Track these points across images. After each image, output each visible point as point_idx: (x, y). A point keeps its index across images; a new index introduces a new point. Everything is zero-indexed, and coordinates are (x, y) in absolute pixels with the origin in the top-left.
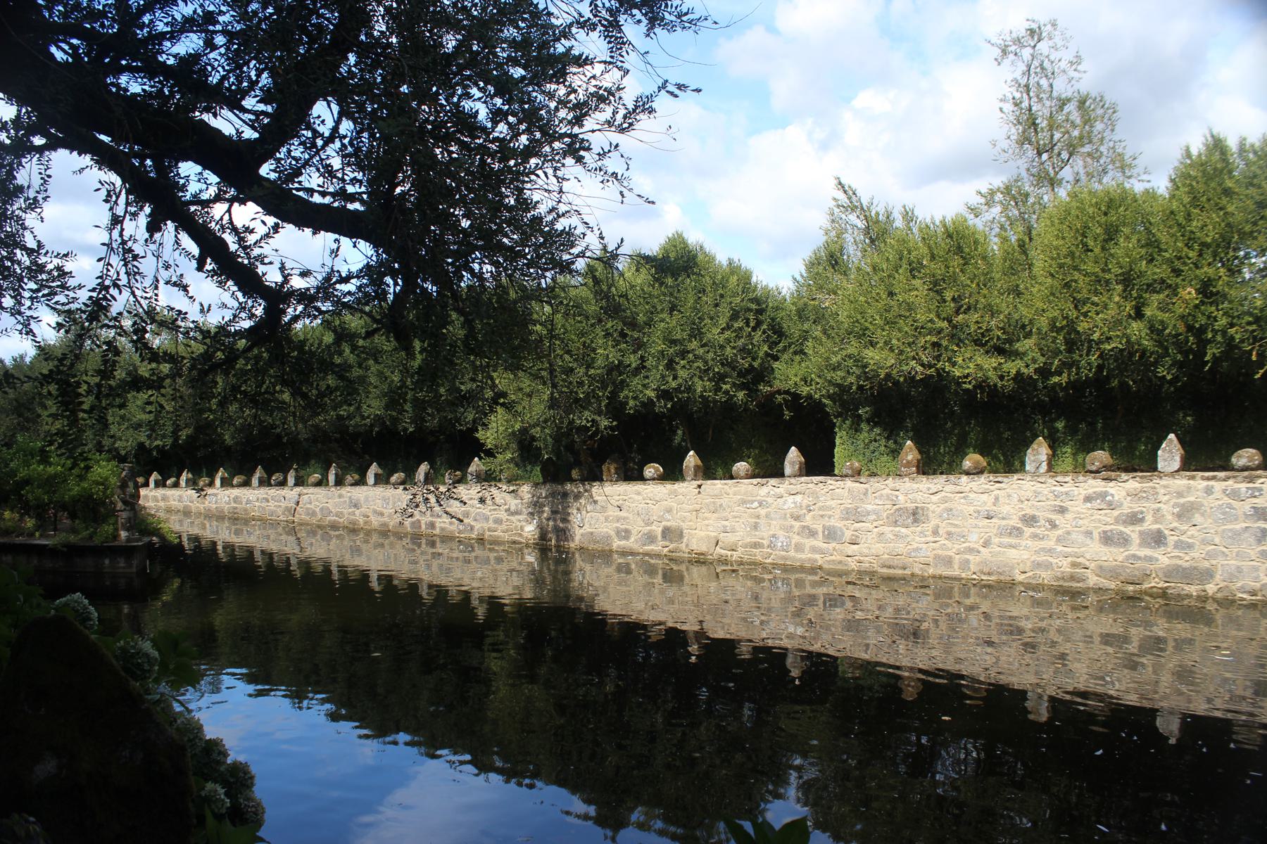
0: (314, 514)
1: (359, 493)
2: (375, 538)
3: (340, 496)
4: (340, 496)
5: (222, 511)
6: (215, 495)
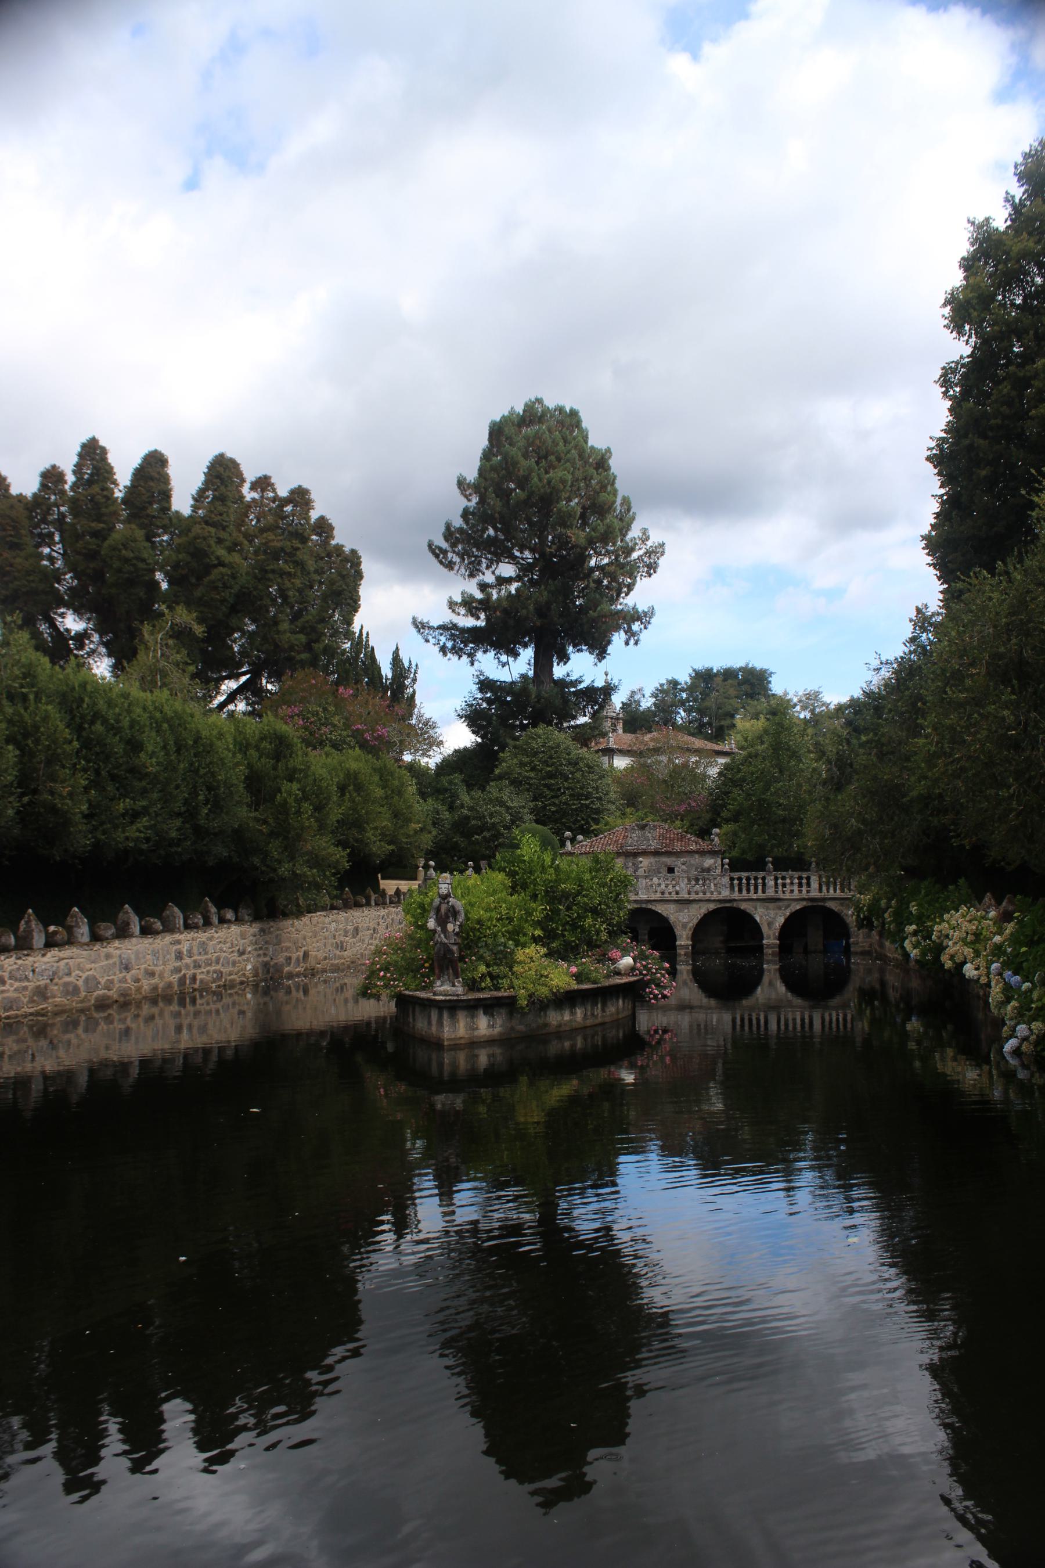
0: (76, 990)
1: (119, 949)
2: (146, 1009)
3: (108, 956)
4: (108, 956)
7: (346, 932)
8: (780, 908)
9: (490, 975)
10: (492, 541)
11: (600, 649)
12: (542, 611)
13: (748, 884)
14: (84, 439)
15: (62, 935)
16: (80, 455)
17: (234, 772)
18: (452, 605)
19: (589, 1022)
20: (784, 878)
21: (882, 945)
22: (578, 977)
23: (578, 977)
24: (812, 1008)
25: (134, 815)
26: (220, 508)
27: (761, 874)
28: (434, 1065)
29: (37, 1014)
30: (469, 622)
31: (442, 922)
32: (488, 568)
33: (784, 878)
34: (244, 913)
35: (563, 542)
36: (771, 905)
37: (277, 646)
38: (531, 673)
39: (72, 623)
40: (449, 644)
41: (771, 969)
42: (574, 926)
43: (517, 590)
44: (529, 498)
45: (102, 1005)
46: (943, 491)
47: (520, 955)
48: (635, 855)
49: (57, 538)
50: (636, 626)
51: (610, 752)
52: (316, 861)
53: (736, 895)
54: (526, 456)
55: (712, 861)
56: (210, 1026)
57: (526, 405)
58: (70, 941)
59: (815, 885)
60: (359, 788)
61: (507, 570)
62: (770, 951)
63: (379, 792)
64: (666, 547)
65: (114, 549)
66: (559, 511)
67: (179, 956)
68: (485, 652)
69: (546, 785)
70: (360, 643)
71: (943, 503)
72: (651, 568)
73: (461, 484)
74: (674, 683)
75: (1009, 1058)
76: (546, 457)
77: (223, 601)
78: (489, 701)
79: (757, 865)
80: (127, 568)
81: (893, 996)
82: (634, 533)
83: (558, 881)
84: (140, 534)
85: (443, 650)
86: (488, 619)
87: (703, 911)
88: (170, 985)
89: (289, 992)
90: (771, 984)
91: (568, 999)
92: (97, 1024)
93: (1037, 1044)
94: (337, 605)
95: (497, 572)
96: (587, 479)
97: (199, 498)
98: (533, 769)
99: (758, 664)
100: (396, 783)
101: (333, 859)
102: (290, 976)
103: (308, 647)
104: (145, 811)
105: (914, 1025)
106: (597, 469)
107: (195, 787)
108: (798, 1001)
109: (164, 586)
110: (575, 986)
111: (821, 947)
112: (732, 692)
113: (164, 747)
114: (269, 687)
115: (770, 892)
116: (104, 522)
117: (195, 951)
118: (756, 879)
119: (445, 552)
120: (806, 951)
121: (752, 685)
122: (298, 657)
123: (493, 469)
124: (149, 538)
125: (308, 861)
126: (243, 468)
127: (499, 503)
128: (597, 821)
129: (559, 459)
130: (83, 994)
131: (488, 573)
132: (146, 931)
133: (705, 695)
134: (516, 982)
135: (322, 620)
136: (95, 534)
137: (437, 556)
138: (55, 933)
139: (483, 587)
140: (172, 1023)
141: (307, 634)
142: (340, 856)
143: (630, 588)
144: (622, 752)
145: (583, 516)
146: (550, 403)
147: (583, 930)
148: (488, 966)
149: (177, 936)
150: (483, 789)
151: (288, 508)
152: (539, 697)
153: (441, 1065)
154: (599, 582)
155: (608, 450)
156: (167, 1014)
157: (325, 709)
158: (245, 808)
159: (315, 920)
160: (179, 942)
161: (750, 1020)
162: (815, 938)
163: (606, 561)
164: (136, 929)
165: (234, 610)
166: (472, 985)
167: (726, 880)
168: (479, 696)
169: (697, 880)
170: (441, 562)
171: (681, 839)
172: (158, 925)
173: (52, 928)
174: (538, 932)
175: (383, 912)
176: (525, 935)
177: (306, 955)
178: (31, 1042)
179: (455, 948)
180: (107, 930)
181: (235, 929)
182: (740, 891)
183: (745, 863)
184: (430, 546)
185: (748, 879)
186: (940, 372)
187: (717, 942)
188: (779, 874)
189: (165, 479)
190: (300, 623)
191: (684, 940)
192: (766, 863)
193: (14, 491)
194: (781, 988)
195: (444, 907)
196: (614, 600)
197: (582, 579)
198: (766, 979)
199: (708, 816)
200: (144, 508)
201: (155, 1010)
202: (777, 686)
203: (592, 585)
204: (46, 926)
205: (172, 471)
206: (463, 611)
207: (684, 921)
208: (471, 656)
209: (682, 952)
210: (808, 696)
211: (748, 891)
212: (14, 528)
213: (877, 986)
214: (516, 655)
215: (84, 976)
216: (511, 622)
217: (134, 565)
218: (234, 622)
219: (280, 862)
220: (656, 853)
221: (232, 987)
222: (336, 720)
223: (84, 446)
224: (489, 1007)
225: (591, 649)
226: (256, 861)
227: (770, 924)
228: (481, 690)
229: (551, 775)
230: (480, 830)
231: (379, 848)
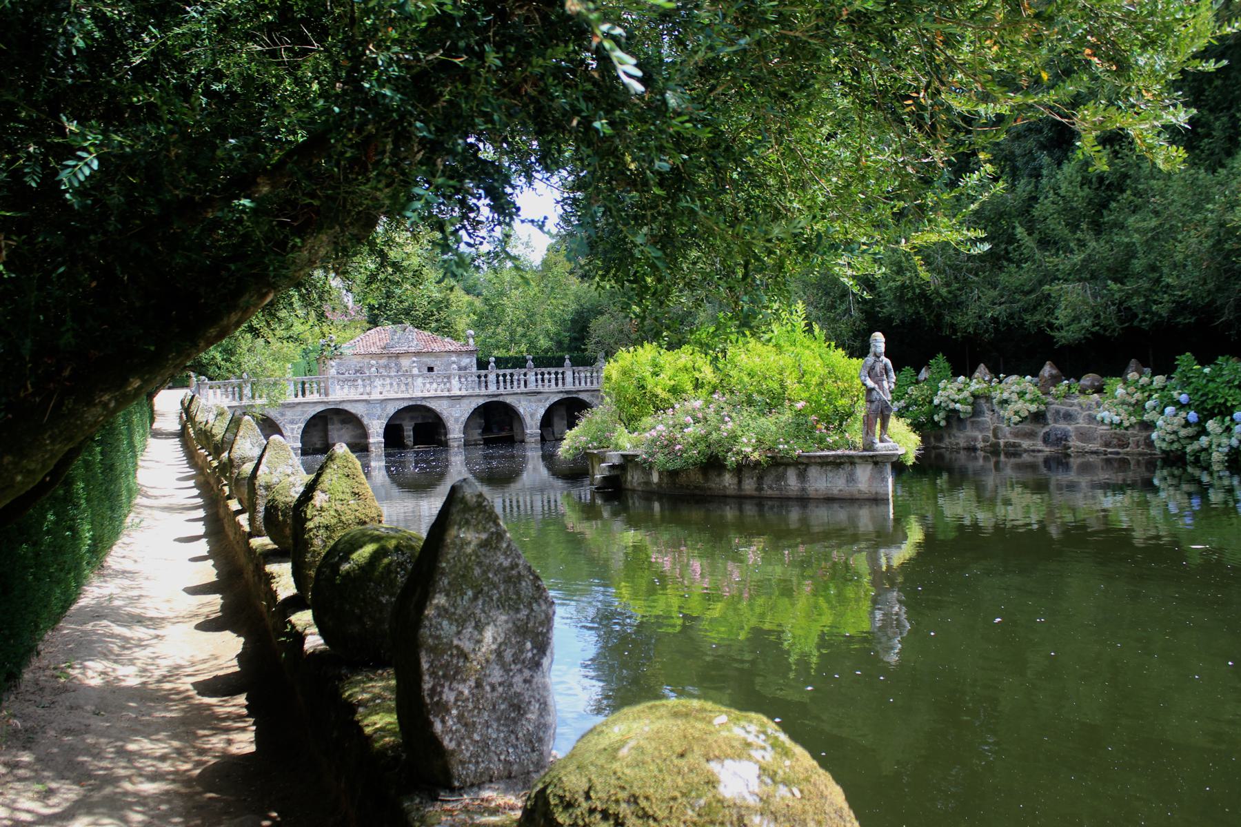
8: (540, 401)
20: (549, 373)
36: (533, 398)
53: (502, 390)
55: (468, 360)
59: (569, 378)
62: (533, 440)
87: (474, 406)
90: (535, 469)
115: (532, 387)
185: (512, 375)
188: (539, 370)
191: (455, 432)
192: (526, 361)
194: (544, 472)
198: (530, 466)
207: (456, 418)
209: (456, 444)
227: (532, 415)
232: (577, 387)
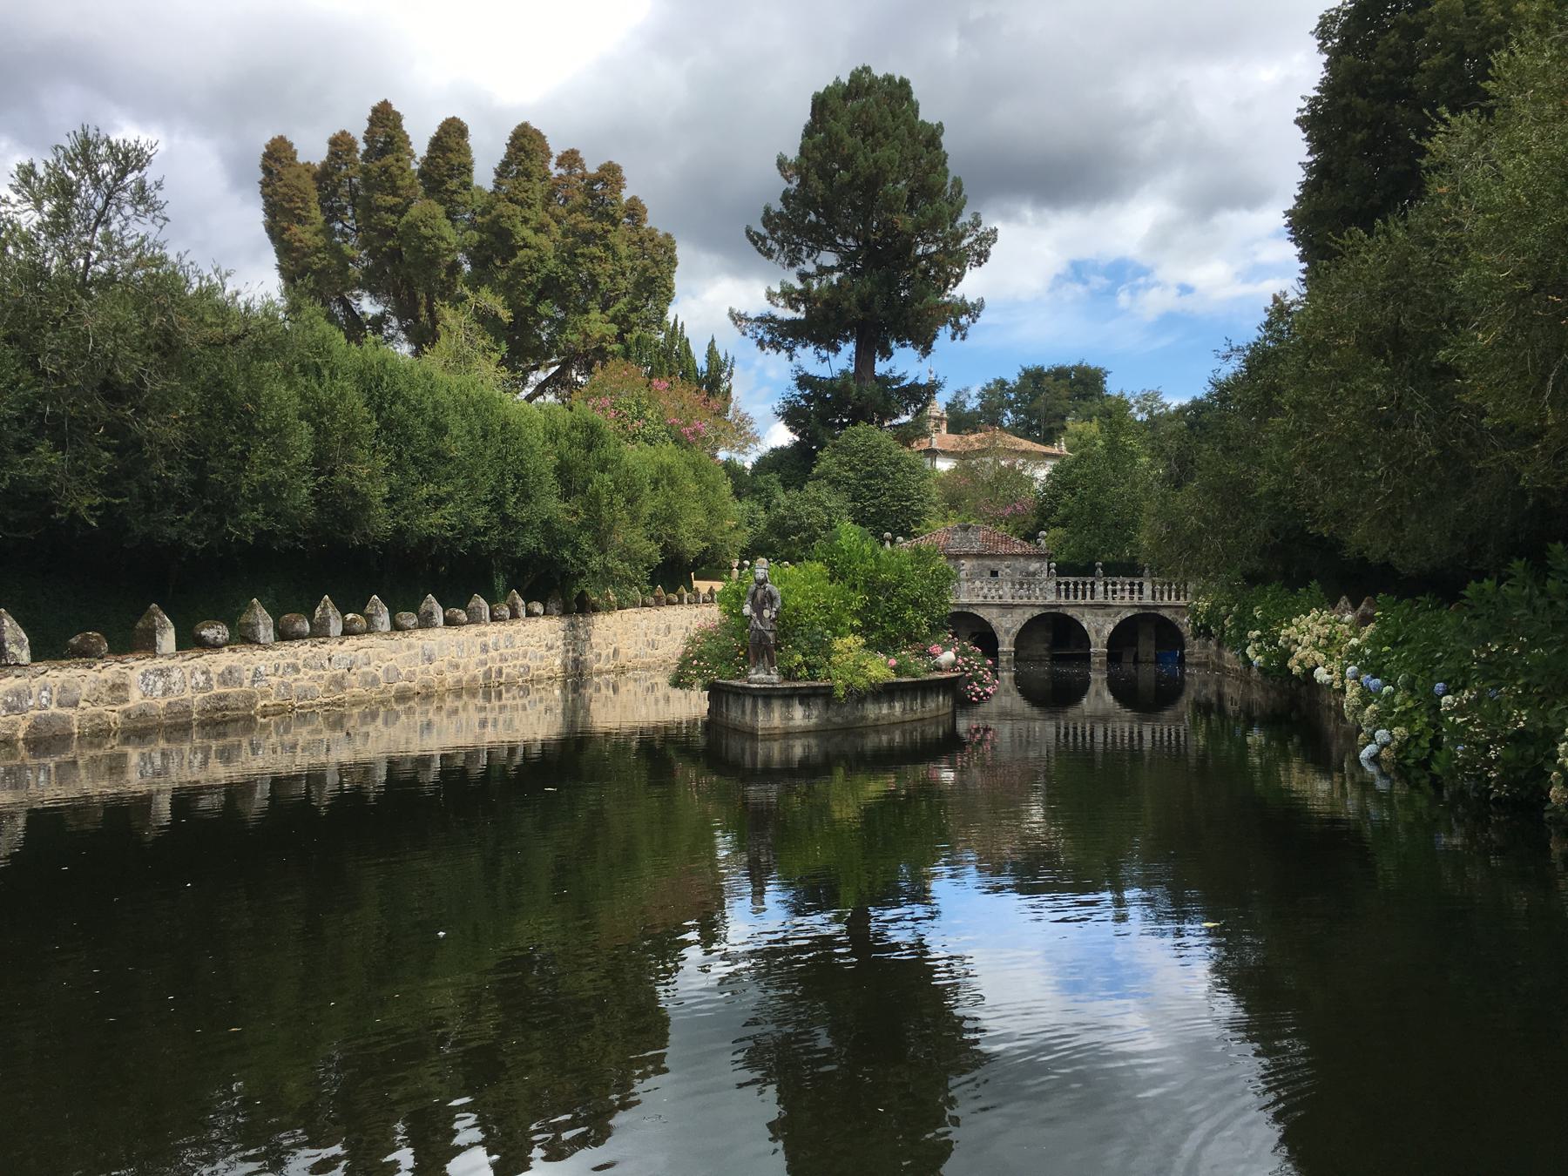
2: (450, 702)
3: (409, 647)
4: (409, 647)
5: (187, 711)
6: (161, 673)
7: (658, 629)
9: (806, 663)
10: (814, 227)
11: (924, 344)
12: (864, 304)
13: (1076, 590)
14: (375, 101)
15: (361, 622)
16: (371, 120)
17: (543, 461)
18: (770, 296)
19: (908, 717)
20: (1114, 584)
21: (1220, 656)
22: (897, 670)
23: (897, 670)
24: (1142, 720)
25: (439, 502)
26: (527, 185)
27: (1089, 580)
28: (747, 757)
29: (333, 704)
30: (787, 314)
31: (758, 608)
32: (809, 256)
33: (1114, 584)
34: (553, 606)
35: (888, 228)
36: (1100, 612)
37: (587, 335)
38: (852, 370)
39: (368, 306)
40: (767, 338)
41: (1098, 676)
42: (894, 618)
43: (839, 280)
44: (853, 179)
45: (402, 697)
46: (1310, 159)
47: (838, 644)
48: (957, 557)
49: (350, 213)
50: (963, 320)
51: (932, 453)
52: (628, 555)
53: (1063, 601)
54: (851, 133)
56: (516, 723)
57: (852, 74)
58: (370, 630)
59: (1147, 590)
60: (672, 482)
61: (829, 258)
63: (693, 487)
64: (999, 234)
65: (412, 226)
66: (886, 194)
67: (485, 649)
68: (804, 346)
69: (867, 486)
70: (675, 333)
71: (1310, 173)
72: (982, 257)
73: (781, 163)
74: (1002, 383)
75: (1364, 764)
76: (872, 134)
77: (530, 286)
78: (808, 398)
79: (1089, 570)
80: (427, 247)
81: (1231, 708)
82: (965, 218)
83: (878, 571)
84: (440, 210)
85: (761, 343)
86: (808, 311)
87: (1028, 616)
88: (474, 678)
89: (598, 690)
90: (1098, 693)
91: (887, 692)
92: (398, 717)
93: (1398, 751)
94: (652, 294)
95: (818, 261)
96: (916, 158)
97: (502, 172)
98: (852, 469)
99: (1093, 363)
100: (711, 478)
101: (646, 552)
102: (600, 673)
103: (620, 338)
104: (450, 496)
105: (1256, 737)
106: (927, 147)
107: (502, 474)
108: (1127, 714)
109: (467, 268)
110: (895, 679)
111: (1152, 657)
112: (1063, 392)
113: (469, 432)
114: (580, 379)
115: (1099, 598)
116: (400, 196)
117: (502, 643)
118: (1084, 584)
119: (764, 239)
120: (1136, 661)
121: (1086, 385)
122: (610, 348)
123: (815, 147)
124: (450, 215)
125: (620, 555)
126: (549, 140)
127: (821, 186)
128: (917, 523)
129: (887, 136)
130: (383, 685)
131: (809, 262)
132: (450, 622)
133: (1034, 396)
134: (833, 672)
135: (635, 310)
136: (391, 210)
137: (755, 243)
138: (353, 621)
139: (803, 277)
140: (476, 718)
141: (619, 324)
142: (652, 550)
143: (959, 277)
144: (946, 454)
145: (911, 200)
146: (879, 72)
147: (903, 623)
148: (804, 655)
149: (482, 628)
150: (801, 489)
151: (598, 187)
152: (860, 395)
153: (754, 754)
154: (926, 272)
155: (940, 125)
156: (471, 707)
157: (638, 403)
158: (555, 499)
159: (625, 617)
160: (484, 634)
161: (1075, 734)
162: (1147, 648)
163: (934, 249)
164: (440, 621)
165: (540, 296)
166: (788, 674)
167: (1052, 584)
168: (798, 392)
169: (1021, 584)
170: (759, 250)
171: (1006, 541)
172: (463, 616)
173: (350, 616)
174: (856, 622)
175: (696, 610)
176: (843, 625)
177: (616, 652)
178: (326, 735)
179: (771, 635)
180: (408, 618)
181: (543, 623)
182: (1067, 597)
183: (1073, 568)
184: (748, 232)
185: (1076, 584)
186: (1318, 21)
187: (1040, 648)
189: (467, 152)
190: (610, 312)
191: (1006, 646)
193: (301, 159)
194: (1109, 698)
195: (760, 593)
196: (941, 291)
197: (907, 269)
198: (1092, 689)
199: (1034, 521)
200: (444, 182)
201: (459, 704)
202: (1112, 387)
203: (919, 275)
204: (343, 614)
205: (475, 140)
206: (782, 303)
207: (1007, 626)
208: (790, 350)
210: (1146, 397)
211: (1076, 597)
212: (303, 200)
213: (1214, 699)
214: (837, 350)
215: (384, 666)
216: (832, 315)
217: (434, 245)
218: (543, 309)
219: (590, 555)
220: (979, 556)
221: (539, 682)
222: (649, 413)
223: (375, 110)
224: (806, 696)
225: (915, 345)
226: (567, 554)
227: (1098, 632)
228: (799, 386)
229: (870, 476)
230: (798, 529)
231: (693, 547)
232: (1158, 602)
